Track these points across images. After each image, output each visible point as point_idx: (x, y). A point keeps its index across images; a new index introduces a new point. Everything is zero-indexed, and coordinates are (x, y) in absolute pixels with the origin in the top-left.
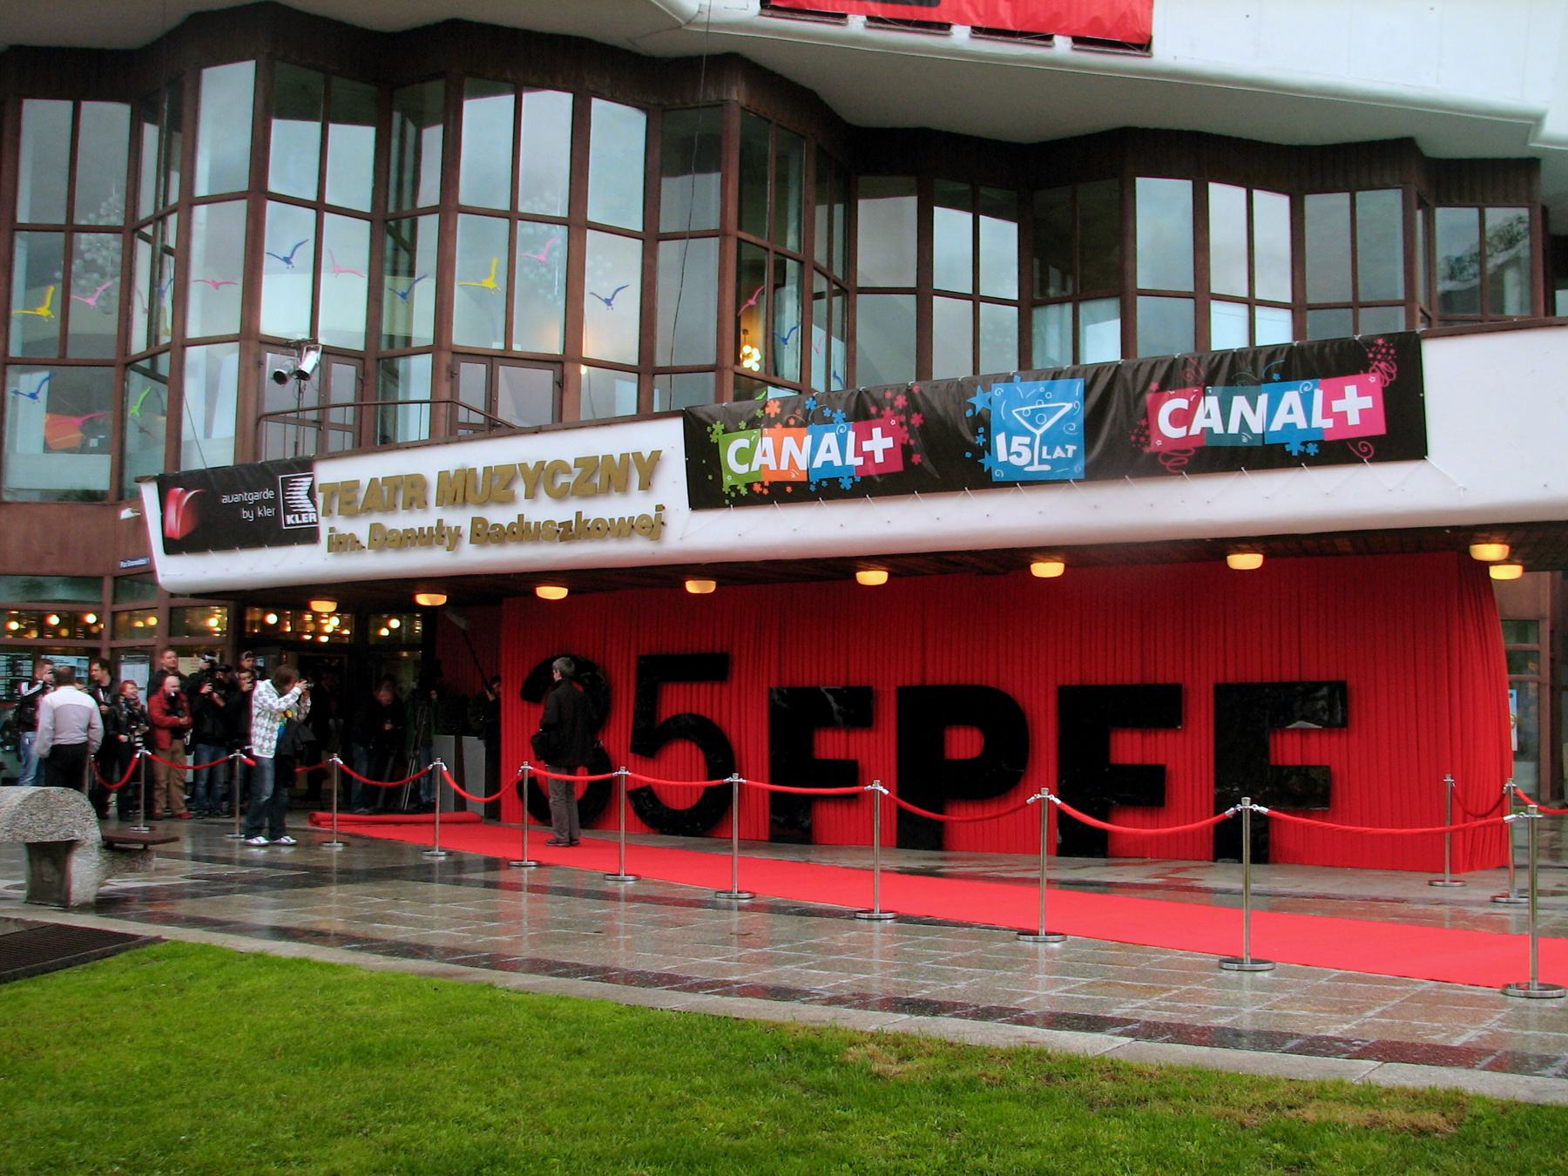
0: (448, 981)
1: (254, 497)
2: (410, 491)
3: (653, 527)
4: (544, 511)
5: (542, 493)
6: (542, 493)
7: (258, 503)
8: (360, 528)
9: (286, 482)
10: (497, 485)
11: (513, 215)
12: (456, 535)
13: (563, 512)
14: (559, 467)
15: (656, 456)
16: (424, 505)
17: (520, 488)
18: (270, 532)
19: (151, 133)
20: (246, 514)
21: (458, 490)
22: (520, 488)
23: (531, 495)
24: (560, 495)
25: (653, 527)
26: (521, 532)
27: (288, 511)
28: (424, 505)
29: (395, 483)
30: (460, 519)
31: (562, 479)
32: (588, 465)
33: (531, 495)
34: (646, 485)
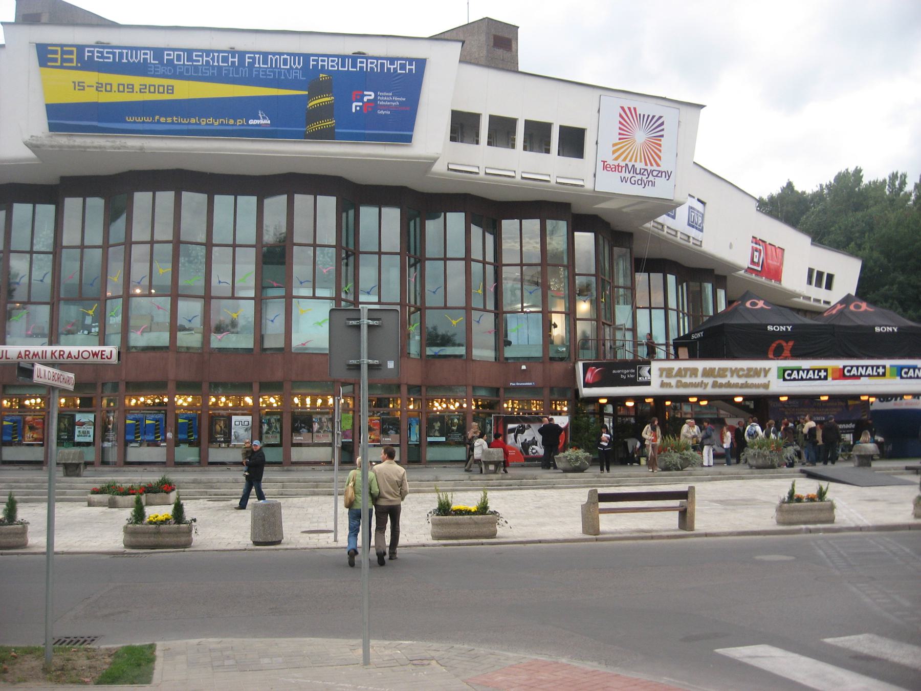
0: (541, 520)
1: (626, 372)
2: (694, 372)
3: (766, 386)
4: (735, 380)
5: (735, 375)
6: (735, 375)
7: (629, 373)
8: (673, 381)
9: (640, 368)
10: (722, 373)
11: (380, 253)
12: (706, 385)
13: (741, 381)
14: (742, 369)
15: (770, 369)
16: (696, 376)
17: (728, 374)
18: (633, 382)
19: (49, 64)
20: (622, 376)
21: (708, 373)
22: (728, 374)
23: (732, 376)
24: (739, 376)
25: (766, 386)
26: (728, 385)
27: (640, 376)
28: (696, 376)
29: (686, 370)
30: (709, 381)
31: (741, 373)
32: (749, 370)
33: (732, 376)
34: (765, 376)
